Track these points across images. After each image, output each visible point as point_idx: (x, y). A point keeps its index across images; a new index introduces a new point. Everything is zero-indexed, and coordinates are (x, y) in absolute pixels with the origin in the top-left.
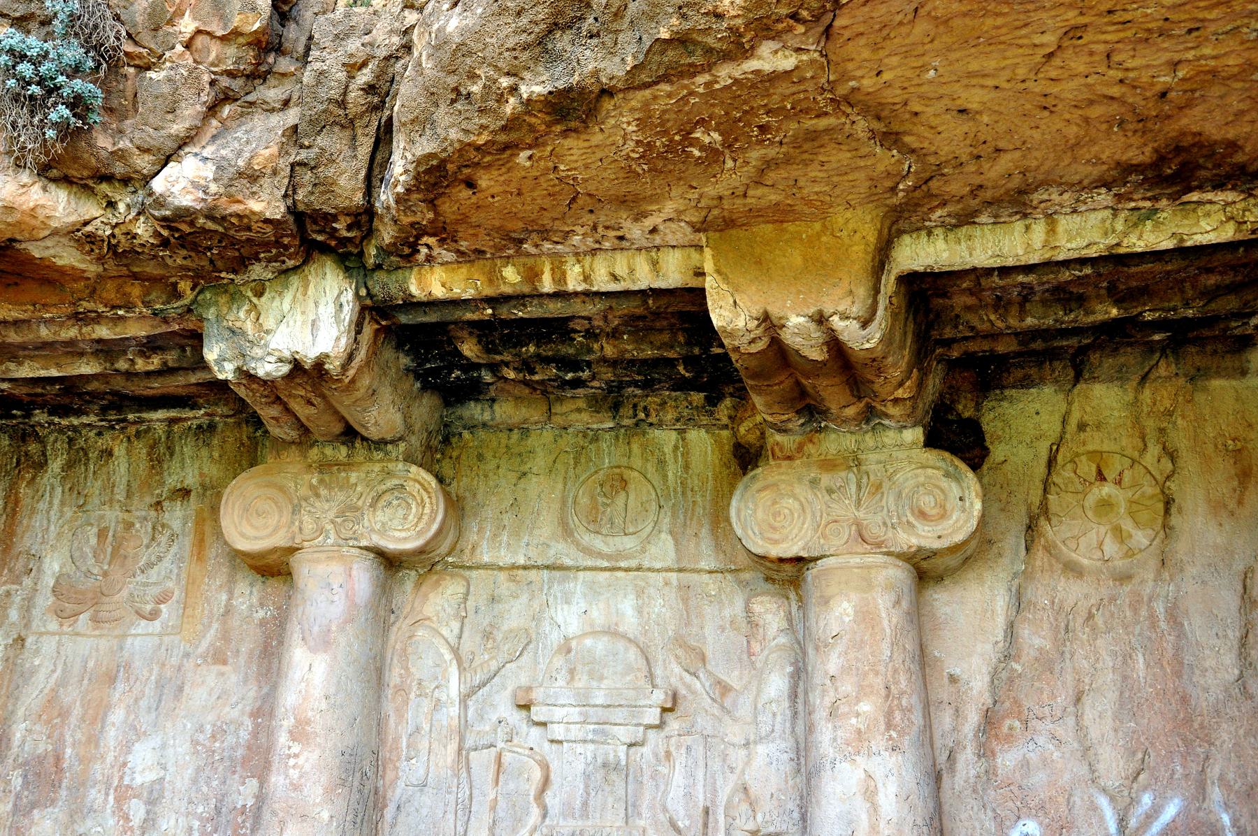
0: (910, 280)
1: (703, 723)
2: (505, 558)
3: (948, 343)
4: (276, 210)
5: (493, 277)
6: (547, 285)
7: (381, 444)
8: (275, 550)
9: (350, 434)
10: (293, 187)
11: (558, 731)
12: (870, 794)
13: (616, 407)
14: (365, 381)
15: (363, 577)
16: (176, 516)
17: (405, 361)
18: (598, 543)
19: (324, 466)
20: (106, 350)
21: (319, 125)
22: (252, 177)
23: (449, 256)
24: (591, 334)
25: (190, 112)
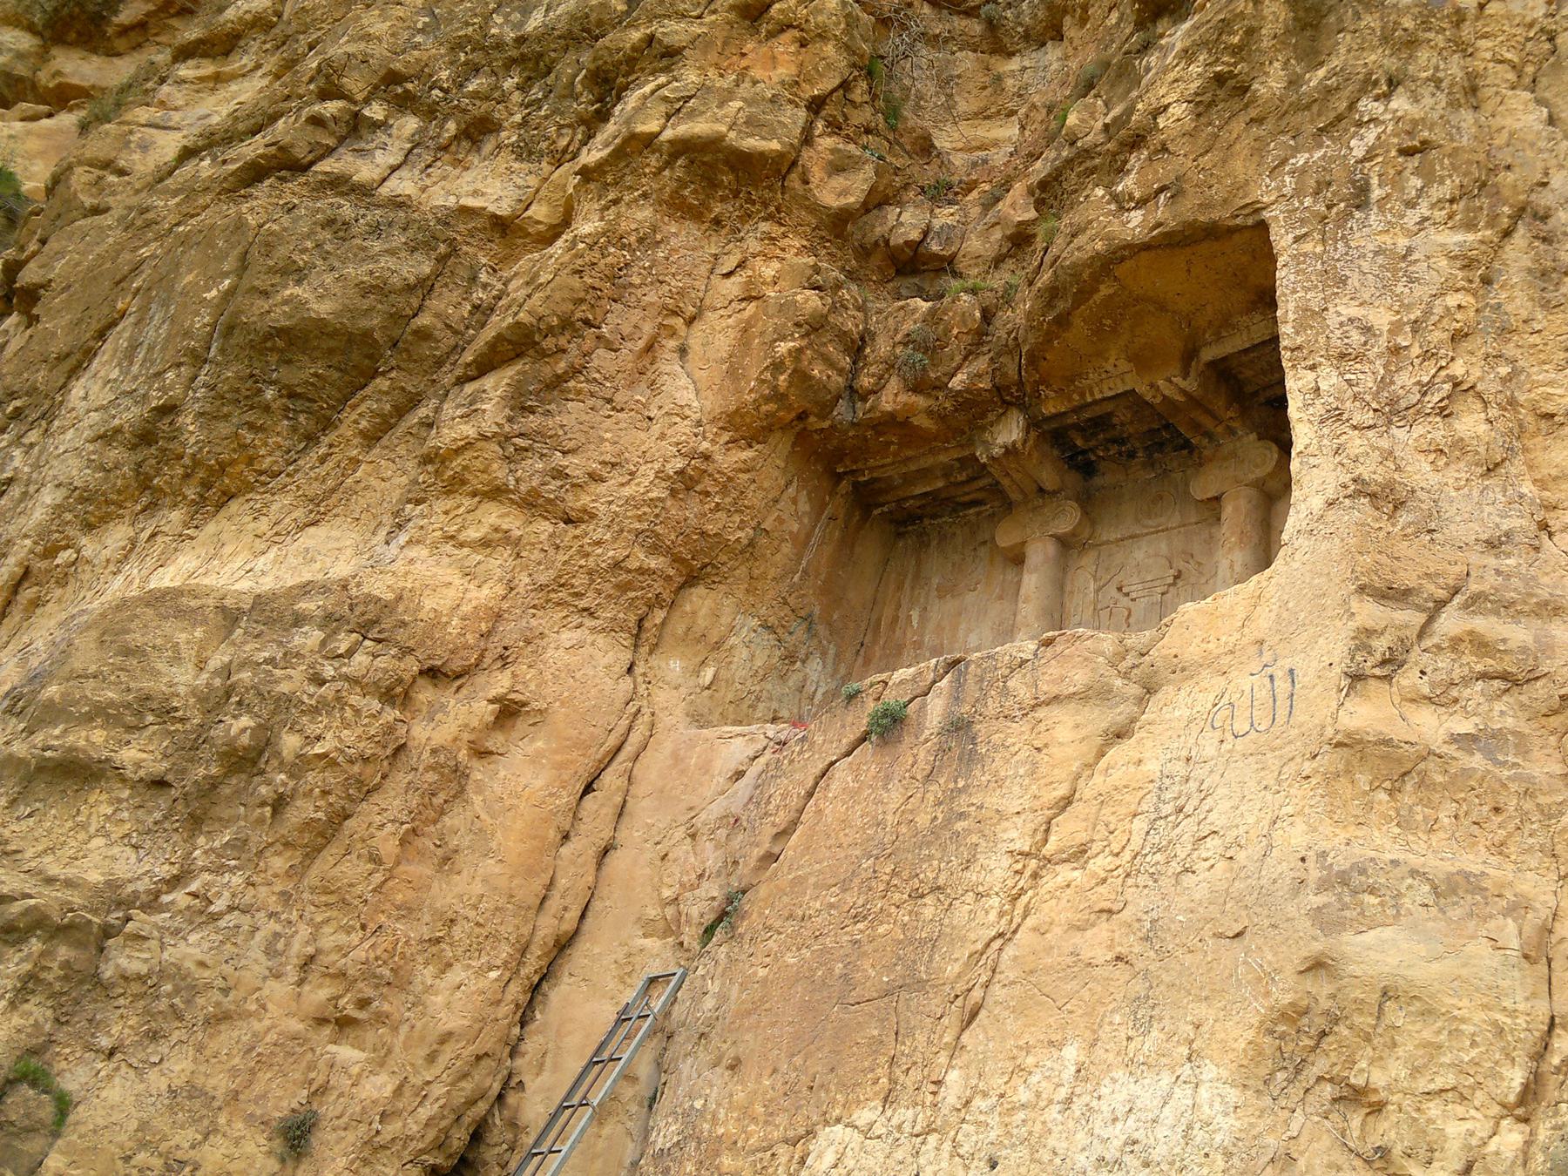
0: (1212, 364)
1: (1193, 580)
2: (1113, 537)
3: (1255, 394)
4: (989, 386)
5: (1070, 399)
6: (1089, 400)
7: (1054, 493)
8: (1016, 545)
9: (1041, 490)
10: (993, 378)
11: (1134, 595)
12: (1231, 567)
13: (1152, 465)
14: (1036, 455)
15: (1051, 548)
16: (983, 551)
17: (1056, 452)
18: (1150, 523)
19: (1035, 509)
20: (947, 472)
21: (999, 354)
22: (980, 376)
23: (1052, 394)
24: (1122, 425)
25: (958, 359)
